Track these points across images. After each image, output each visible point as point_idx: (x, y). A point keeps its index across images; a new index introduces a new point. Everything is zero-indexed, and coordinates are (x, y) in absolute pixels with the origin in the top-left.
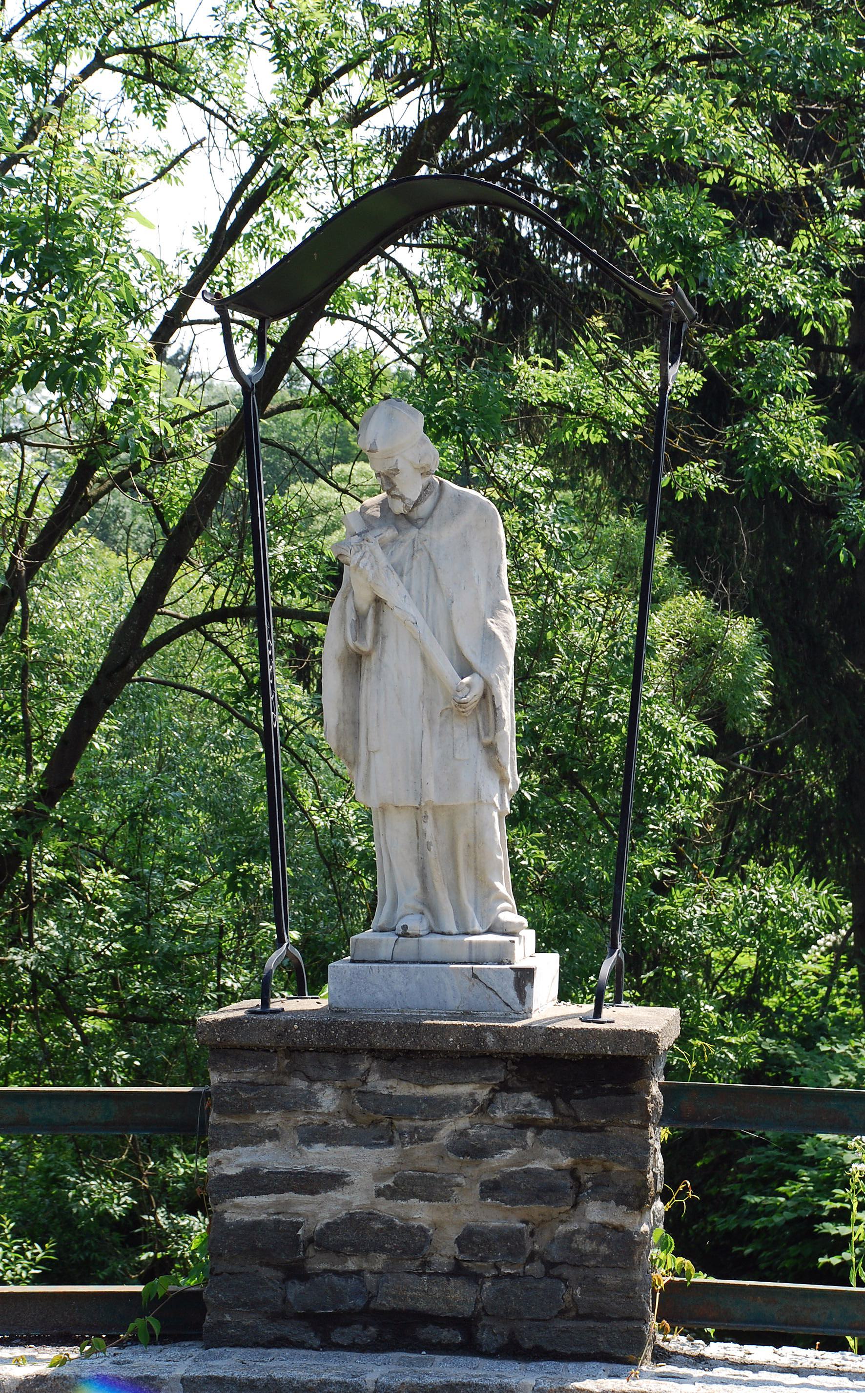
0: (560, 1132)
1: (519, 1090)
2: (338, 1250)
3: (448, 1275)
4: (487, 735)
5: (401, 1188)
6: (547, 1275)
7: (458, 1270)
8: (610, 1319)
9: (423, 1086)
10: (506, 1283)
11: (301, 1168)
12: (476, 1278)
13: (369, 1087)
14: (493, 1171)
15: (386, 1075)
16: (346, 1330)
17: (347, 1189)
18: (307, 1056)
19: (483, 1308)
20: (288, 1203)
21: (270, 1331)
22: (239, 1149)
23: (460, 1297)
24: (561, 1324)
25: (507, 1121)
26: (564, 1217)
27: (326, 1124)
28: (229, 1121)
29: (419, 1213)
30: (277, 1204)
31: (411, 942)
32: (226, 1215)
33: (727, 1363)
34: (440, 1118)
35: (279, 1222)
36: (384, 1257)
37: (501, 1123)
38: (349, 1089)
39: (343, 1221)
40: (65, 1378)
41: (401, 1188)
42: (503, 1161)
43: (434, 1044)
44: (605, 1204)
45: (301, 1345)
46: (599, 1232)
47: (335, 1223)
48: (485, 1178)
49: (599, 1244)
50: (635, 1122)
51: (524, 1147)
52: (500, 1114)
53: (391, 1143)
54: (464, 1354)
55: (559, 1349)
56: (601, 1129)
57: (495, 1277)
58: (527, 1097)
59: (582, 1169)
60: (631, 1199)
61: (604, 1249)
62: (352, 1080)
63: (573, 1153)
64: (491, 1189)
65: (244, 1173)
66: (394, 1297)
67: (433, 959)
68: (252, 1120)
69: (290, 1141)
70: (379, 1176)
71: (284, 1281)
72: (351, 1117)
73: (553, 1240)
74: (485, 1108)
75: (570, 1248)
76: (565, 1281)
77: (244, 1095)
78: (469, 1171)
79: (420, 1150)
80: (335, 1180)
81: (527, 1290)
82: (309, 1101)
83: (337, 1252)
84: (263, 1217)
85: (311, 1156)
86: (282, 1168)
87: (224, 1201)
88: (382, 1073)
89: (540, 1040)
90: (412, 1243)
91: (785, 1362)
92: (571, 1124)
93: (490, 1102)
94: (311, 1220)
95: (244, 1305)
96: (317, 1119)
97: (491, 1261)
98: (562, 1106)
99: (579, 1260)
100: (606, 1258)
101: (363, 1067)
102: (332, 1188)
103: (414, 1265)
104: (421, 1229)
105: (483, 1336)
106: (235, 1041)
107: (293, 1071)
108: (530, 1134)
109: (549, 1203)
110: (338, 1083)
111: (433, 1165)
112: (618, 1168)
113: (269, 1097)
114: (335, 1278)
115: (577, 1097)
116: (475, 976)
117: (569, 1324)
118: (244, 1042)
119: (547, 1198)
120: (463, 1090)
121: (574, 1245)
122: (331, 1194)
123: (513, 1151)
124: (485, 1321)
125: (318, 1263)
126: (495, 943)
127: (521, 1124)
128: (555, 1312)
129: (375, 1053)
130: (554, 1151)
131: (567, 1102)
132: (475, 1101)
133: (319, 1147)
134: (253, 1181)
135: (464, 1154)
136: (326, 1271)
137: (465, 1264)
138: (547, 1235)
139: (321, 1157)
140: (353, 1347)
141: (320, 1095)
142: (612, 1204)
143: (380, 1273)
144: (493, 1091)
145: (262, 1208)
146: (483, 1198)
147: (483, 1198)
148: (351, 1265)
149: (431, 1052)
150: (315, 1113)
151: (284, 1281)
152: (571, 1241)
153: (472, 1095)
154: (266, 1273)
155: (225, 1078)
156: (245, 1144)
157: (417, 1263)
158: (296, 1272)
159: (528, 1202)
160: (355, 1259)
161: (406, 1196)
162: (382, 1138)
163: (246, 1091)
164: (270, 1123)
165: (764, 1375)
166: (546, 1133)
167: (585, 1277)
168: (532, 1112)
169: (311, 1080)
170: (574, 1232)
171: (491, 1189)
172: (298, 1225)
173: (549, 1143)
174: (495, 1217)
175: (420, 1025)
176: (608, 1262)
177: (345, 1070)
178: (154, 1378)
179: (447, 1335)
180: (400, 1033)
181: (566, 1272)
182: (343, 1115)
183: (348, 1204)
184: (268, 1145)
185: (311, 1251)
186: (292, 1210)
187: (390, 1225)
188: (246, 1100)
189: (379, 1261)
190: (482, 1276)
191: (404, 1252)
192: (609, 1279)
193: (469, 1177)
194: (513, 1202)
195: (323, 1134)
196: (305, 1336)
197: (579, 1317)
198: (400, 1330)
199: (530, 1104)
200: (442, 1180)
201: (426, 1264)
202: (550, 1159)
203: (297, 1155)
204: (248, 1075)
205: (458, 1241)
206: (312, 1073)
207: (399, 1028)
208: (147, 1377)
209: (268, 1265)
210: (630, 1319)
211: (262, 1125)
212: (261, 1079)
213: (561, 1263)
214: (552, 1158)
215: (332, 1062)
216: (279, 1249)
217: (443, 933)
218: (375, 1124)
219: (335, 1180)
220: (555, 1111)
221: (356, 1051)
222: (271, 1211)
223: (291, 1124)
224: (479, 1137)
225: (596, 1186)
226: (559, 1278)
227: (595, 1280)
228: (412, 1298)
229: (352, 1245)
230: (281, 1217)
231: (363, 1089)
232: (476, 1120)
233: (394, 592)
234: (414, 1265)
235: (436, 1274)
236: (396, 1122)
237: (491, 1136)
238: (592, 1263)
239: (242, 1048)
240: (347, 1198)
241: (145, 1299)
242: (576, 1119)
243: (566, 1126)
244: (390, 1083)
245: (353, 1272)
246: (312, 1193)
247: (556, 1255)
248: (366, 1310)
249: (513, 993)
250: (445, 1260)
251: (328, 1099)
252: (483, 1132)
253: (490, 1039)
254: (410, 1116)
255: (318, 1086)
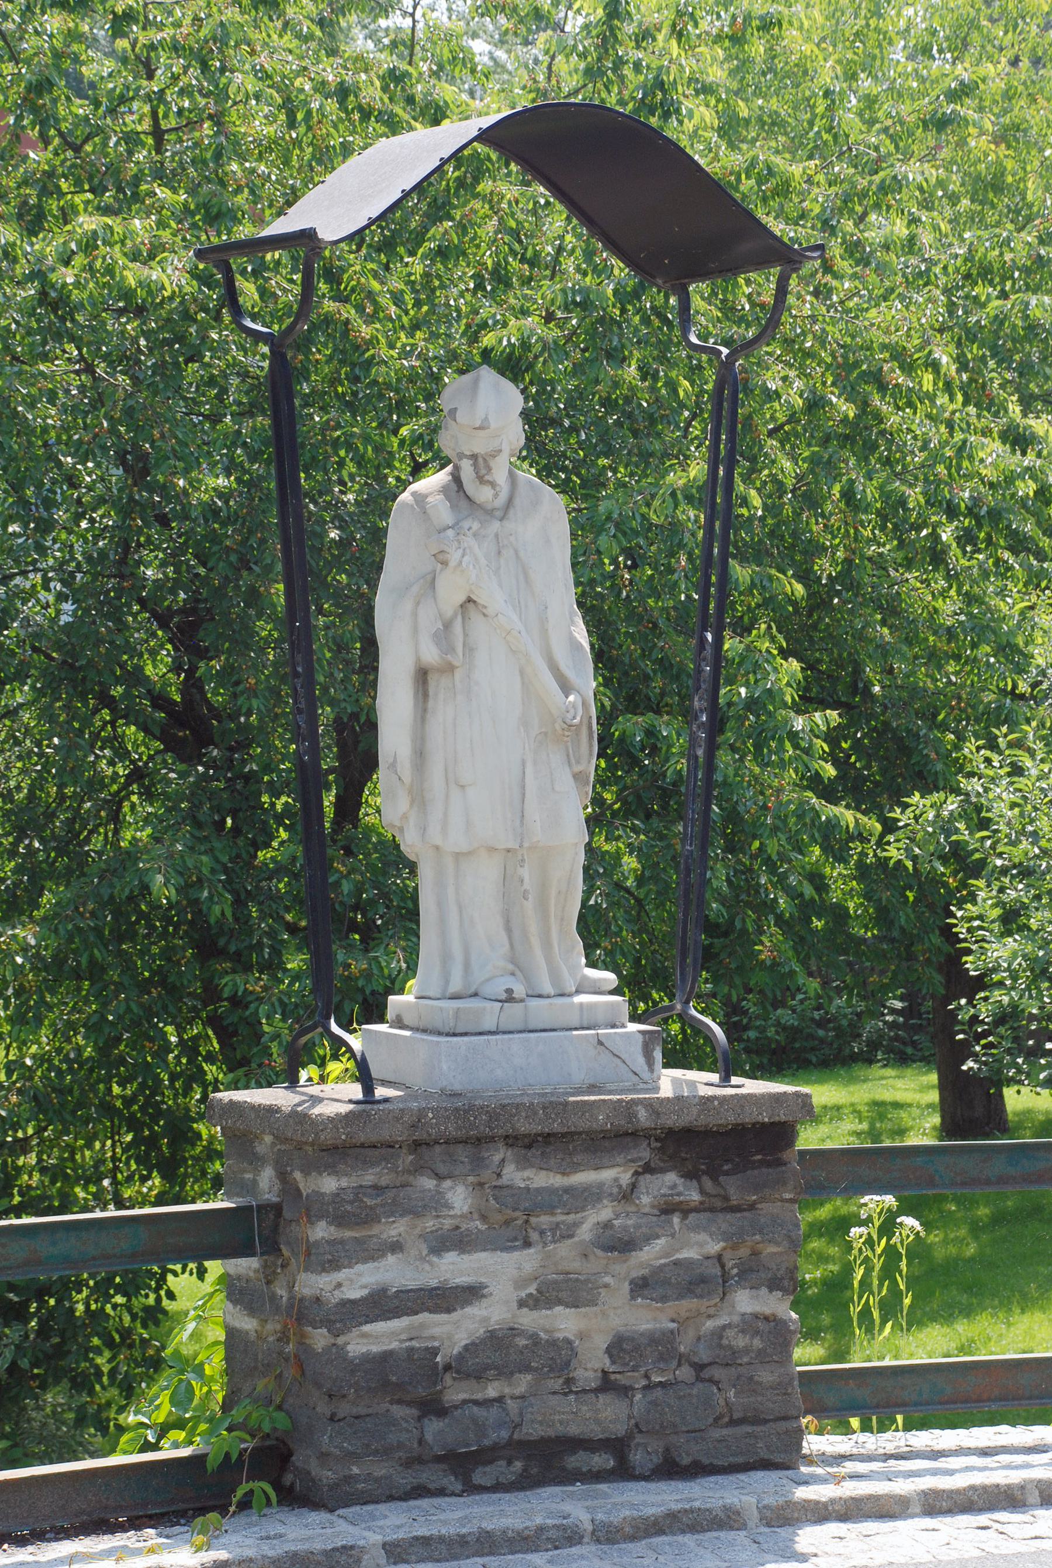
0: (708, 1214)
1: (663, 1171)
2: (479, 1376)
3: (597, 1391)
4: (578, 762)
5: (544, 1296)
6: (699, 1379)
7: (607, 1384)
8: (766, 1421)
9: (564, 1174)
10: (658, 1393)
11: (434, 1283)
12: (625, 1391)
13: (504, 1180)
14: (641, 1265)
15: (523, 1163)
16: (488, 1469)
17: (485, 1302)
18: (438, 1149)
19: (637, 1425)
20: (422, 1326)
21: (406, 1480)
22: (359, 1267)
23: (610, 1415)
24: (717, 1433)
25: (653, 1207)
26: (712, 1311)
27: (457, 1228)
28: (348, 1234)
29: (565, 1322)
30: (410, 1328)
31: (515, 1009)
32: (349, 1348)
33: (960, 1451)
34: (583, 1209)
35: (412, 1349)
36: (529, 1377)
37: (647, 1210)
38: (481, 1185)
39: (483, 1341)
40: (251, 1560)
41: (544, 1296)
42: (651, 1254)
43: (582, 1124)
44: (754, 1292)
45: (441, 1492)
46: (752, 1323)
47: (473, 1344)
48: (634, 1274)
49: (752, 1337)
50: (787, 1196)
51: (673, 1235)
52: (645, 1200)
53: (527, 1244)
54: (659, 1480)
55: (715, 1462)
56: (752, 1207)
57: (646, 1388)
58: (671, 1177)
59: (727, 1255)
60: (786, 1283)
61: (757, 1343)
62: (487, 1175)
63: (726, 1237)
64: (641, 1286)
65: (371, 1295)
66: (541, 1423)
67: (541, 1026)
68: (375, 1230)
69: (414, 1252)
70: (520, 1283)
71: (419, 1419)
72: (484, 1218)
73: (699, 1339)
74: (627, 1194)
75: (720, 1346)
76: (717, 1383)
77: (369, 1202)
78: (619, 1268)
79: (564, 1250)
80: (472, 1293)
81: (680, 1398)
82: (437, 1204)
83: (478, 1378)
84: (394, 1345)
85: (443, 1268)
86: (412, 1284)
87: (349, 1330)
88: (518, 1163)
89: (695, 1111)
90: (556, 1359)
91: (890, 1448)
92: (719, 1204)
93: (634, 1186)
94: (447, 1343)
95: (376, 1452)
96: (448, 1223)
97: (642, 1370)
98: (708, 1183)
99: (730, 1359)
100: (760, 1352)
101: (497, 1158)
102: (467, 1302)
103: (557, 1384)
104: (568, 1342)
105: (637, 1457)
106: (362, 1138)
107: (418, 1169)
108: (676, 1220)
109: (701, 1297)
110: (471, 1179)
111: (576, 1265)
112: (772, 1249)
113: (396, 1202)
114: (475, 1409)
115: (727, 1173)
116: (600, 1043)
117: (725, 1432)
118: (374, 1138)
119: (699, 1291)
120: (607, 1175)
121: (725, 1342)
122: (469, 1310)
123: (662, 1241)
124: (639, 1439)
125: (456, 1393)
126: (607, 1003)
127: (667, 1209)
128: (711, 1420)
129: (512, 1140)
130: (703, 1237)
131: (715, 1179)
132: (620, 1187)
133: (451, 1257)
134: (382, 1304)
135: (611, 1249)
136: (465, 1402)
137: (613, 1377)
138: (691, 1334)
139: (454, 1268)
140: (497, 1488)
141: (449, 1195)
142: (764, 1290)
143: (522, 1397)
144: (636, 1173)
145: (394, 1334)
146: (633, 1298)
147: (633, 1298)
148: (492, 1392)
149: (572, 1134)
150: (445, 1217)
151: (419, 1419)
152: (721, 1337)
153: (616, 1180)
154: (399, 1411)
155: (344, 1183)
156: (365, 1261)
157: (561, 1381)
158: (433, 1407)
159: (680, 1297)
160: (496, 1384)
161: (550, 1304)
162: (516, 1239)
163: (371, 1196)
164: (393, 1233)
165: (850, 1467)
166: (692, 1217)
167: (738, 1378)
168: (679, 1194)
169: (440, 1177)
170: (724, 1328)
171: (641, 1286)
172: (435, 1352)
173: (696, 1228)
174: (645, 1319)
175: (566, 1104)
176: (762, 1357)
177: (478, 1163)
178: (352, 1547)
179: (603, 1461)
180: (546, 1114)
181: (717, 1373)
182: (476, 1216)
183: (485, 1320)
184: (391, 1259)
185: (448, 1379)
186: (427, 1333)
187: (534, 1338)
188: (371, 1208)
189: (523, 1383)
190: (633, 1389)
191: (551, 1370)
192: (766, 1376)
193: (617, 1275)
194: (664, 1299)
195: (457, 1240)
196: (445, 1481)
197: (733, 1423)
198: (547, 1461)
199: (674, 1186)
200: (587, 1281)
201: (569, 1381)
202: (698, 1245)
203: (427, 1267)
204: (369, 1178)
205: (608, 1351)
206: (442, 1169)
207: (544, 1108)
208: (344, 1547)
209: (400, 1402)
210: (785, 1418)
211: (384, 1236)
212: (384, 1181)
213: (710, 1364)
214: (701, 1245)
215: (462, 1153)
216: (417, 1382)
217: (540, 996)
218: (512, 1223)
219: (472, 1293)
220: (702, 1192)
221: (492, 1139)
222: (403, 1337)
223: (417, 1231)
224: (625, 1228)
225: (742, 1274)
226: (711, 1380)
227: (751, 1378)
228: (561, 1422)
229: (496, 1368)
230: (415, 1344)
231: (499, 1183)
232: (619, 1209)
233: (494, 596)
234: (557, 1384)
235: (584, 1391)
236: (533, 1220)
237: (637, 1227)
238: (745, 1360)
239: (362, 1146)
240: (484, 1313)
241: (211, 1464)
242: (726, 1198)
243: (718, 1206)
244: (527, 1173)
245: (495, 1400)
246: (449, 1310)
247: (704, 1355)
248: (510, 1443)
249: (641, 1060)
250: (590, 1374)
251: (459, 1198)
252: (630, 1222)
253: (642, 1114)
254: (551, 1210)
255: (448, 1183)
